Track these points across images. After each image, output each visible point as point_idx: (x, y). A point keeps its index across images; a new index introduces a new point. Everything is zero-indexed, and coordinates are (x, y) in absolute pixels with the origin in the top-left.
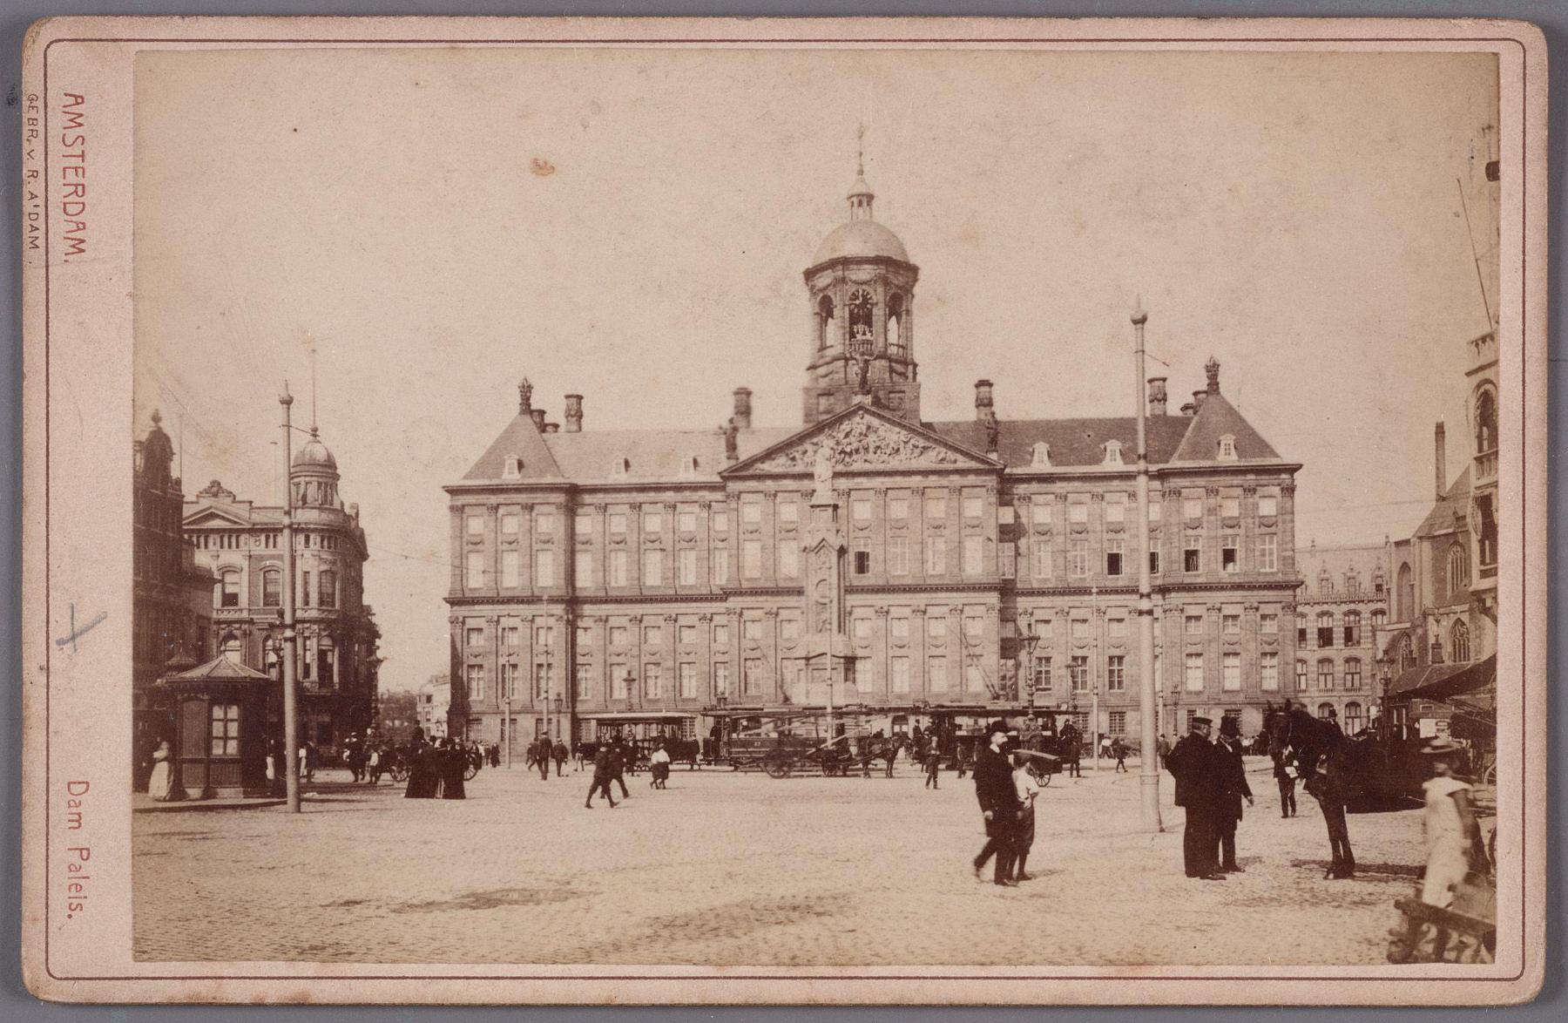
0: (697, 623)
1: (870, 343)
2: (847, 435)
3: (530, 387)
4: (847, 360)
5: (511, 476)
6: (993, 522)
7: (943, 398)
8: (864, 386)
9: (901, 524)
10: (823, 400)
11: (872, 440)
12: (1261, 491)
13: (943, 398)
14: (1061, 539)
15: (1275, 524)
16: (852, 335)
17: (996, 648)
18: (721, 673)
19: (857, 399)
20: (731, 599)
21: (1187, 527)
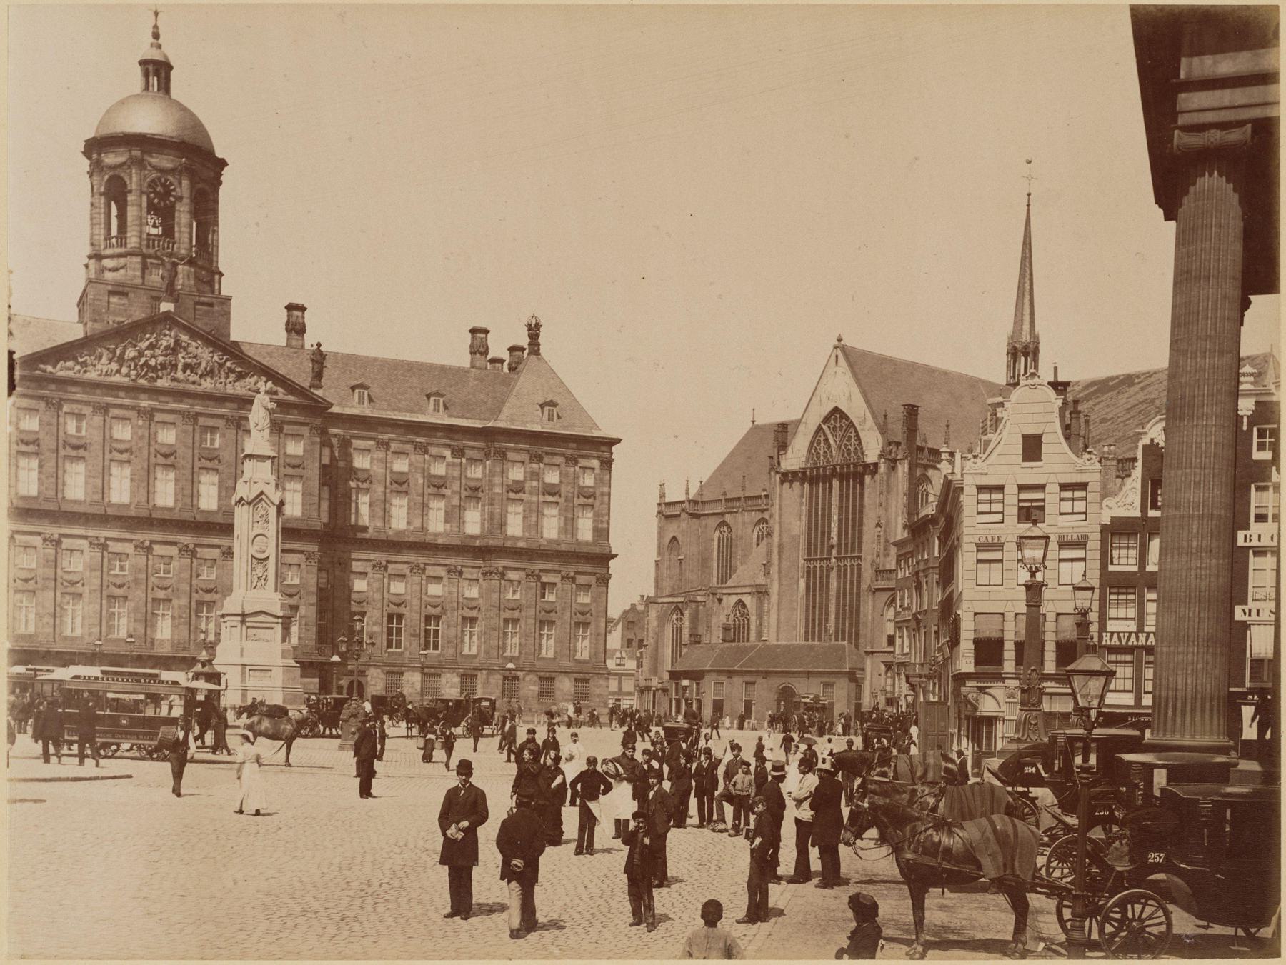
6: (317, 465)
8: (171, 291)
11: (182, 358)
12: (583, 462)
14: (380, 489)
15: (592, 496)
17: (314, 599)
19: (166, 307)
21: (510, 489)
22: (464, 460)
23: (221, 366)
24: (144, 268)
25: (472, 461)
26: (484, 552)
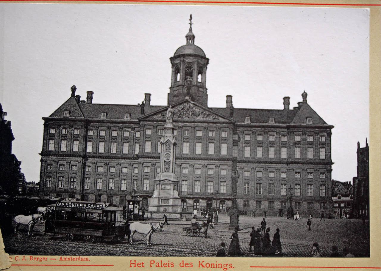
0: (127, 166)
1: (191, 81)
2: (182, 109)
3: (75, 89)
4: (183, 86)
5: (66, 114)
6: (231, 139)
7: (216, 100)
8: (188, 94)
9: (199, 138)
10: (175, 98)
13: (216, 100)
16: (186, 79)
18: (135, 183)
19: (187, 98)
20: (140, 159)
21: (295, 144)
22: (281, 136)
23: (202, 113)
24: (183, 88)
25: (284, 136)
26: (288, 163)
